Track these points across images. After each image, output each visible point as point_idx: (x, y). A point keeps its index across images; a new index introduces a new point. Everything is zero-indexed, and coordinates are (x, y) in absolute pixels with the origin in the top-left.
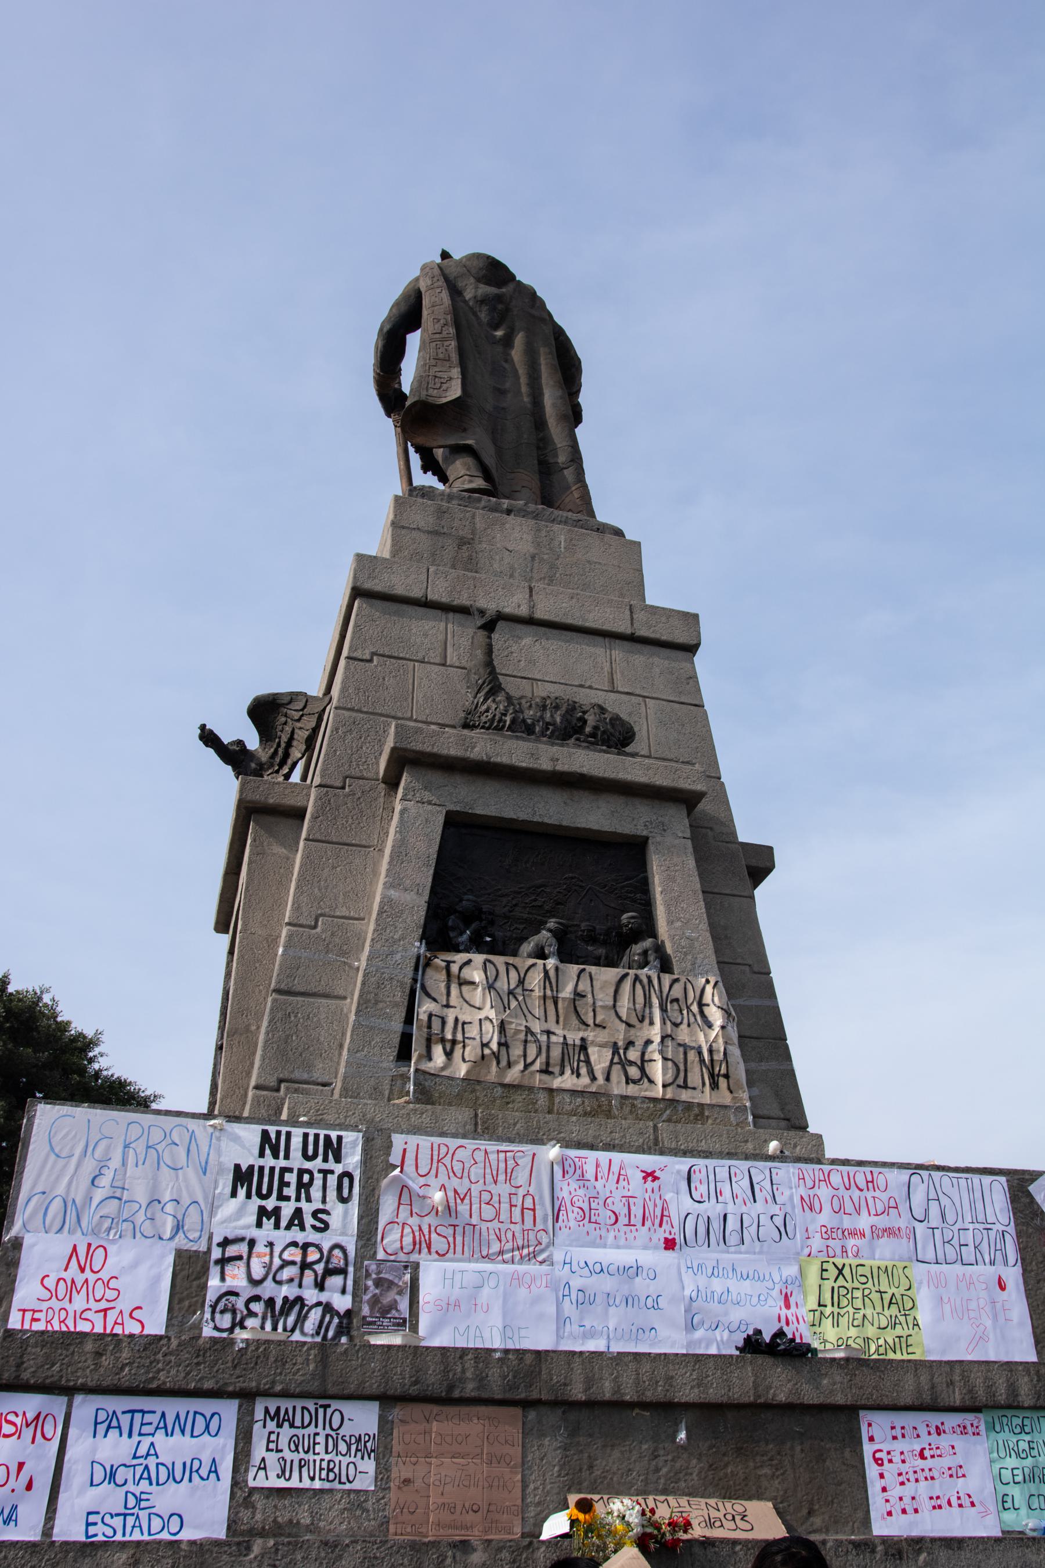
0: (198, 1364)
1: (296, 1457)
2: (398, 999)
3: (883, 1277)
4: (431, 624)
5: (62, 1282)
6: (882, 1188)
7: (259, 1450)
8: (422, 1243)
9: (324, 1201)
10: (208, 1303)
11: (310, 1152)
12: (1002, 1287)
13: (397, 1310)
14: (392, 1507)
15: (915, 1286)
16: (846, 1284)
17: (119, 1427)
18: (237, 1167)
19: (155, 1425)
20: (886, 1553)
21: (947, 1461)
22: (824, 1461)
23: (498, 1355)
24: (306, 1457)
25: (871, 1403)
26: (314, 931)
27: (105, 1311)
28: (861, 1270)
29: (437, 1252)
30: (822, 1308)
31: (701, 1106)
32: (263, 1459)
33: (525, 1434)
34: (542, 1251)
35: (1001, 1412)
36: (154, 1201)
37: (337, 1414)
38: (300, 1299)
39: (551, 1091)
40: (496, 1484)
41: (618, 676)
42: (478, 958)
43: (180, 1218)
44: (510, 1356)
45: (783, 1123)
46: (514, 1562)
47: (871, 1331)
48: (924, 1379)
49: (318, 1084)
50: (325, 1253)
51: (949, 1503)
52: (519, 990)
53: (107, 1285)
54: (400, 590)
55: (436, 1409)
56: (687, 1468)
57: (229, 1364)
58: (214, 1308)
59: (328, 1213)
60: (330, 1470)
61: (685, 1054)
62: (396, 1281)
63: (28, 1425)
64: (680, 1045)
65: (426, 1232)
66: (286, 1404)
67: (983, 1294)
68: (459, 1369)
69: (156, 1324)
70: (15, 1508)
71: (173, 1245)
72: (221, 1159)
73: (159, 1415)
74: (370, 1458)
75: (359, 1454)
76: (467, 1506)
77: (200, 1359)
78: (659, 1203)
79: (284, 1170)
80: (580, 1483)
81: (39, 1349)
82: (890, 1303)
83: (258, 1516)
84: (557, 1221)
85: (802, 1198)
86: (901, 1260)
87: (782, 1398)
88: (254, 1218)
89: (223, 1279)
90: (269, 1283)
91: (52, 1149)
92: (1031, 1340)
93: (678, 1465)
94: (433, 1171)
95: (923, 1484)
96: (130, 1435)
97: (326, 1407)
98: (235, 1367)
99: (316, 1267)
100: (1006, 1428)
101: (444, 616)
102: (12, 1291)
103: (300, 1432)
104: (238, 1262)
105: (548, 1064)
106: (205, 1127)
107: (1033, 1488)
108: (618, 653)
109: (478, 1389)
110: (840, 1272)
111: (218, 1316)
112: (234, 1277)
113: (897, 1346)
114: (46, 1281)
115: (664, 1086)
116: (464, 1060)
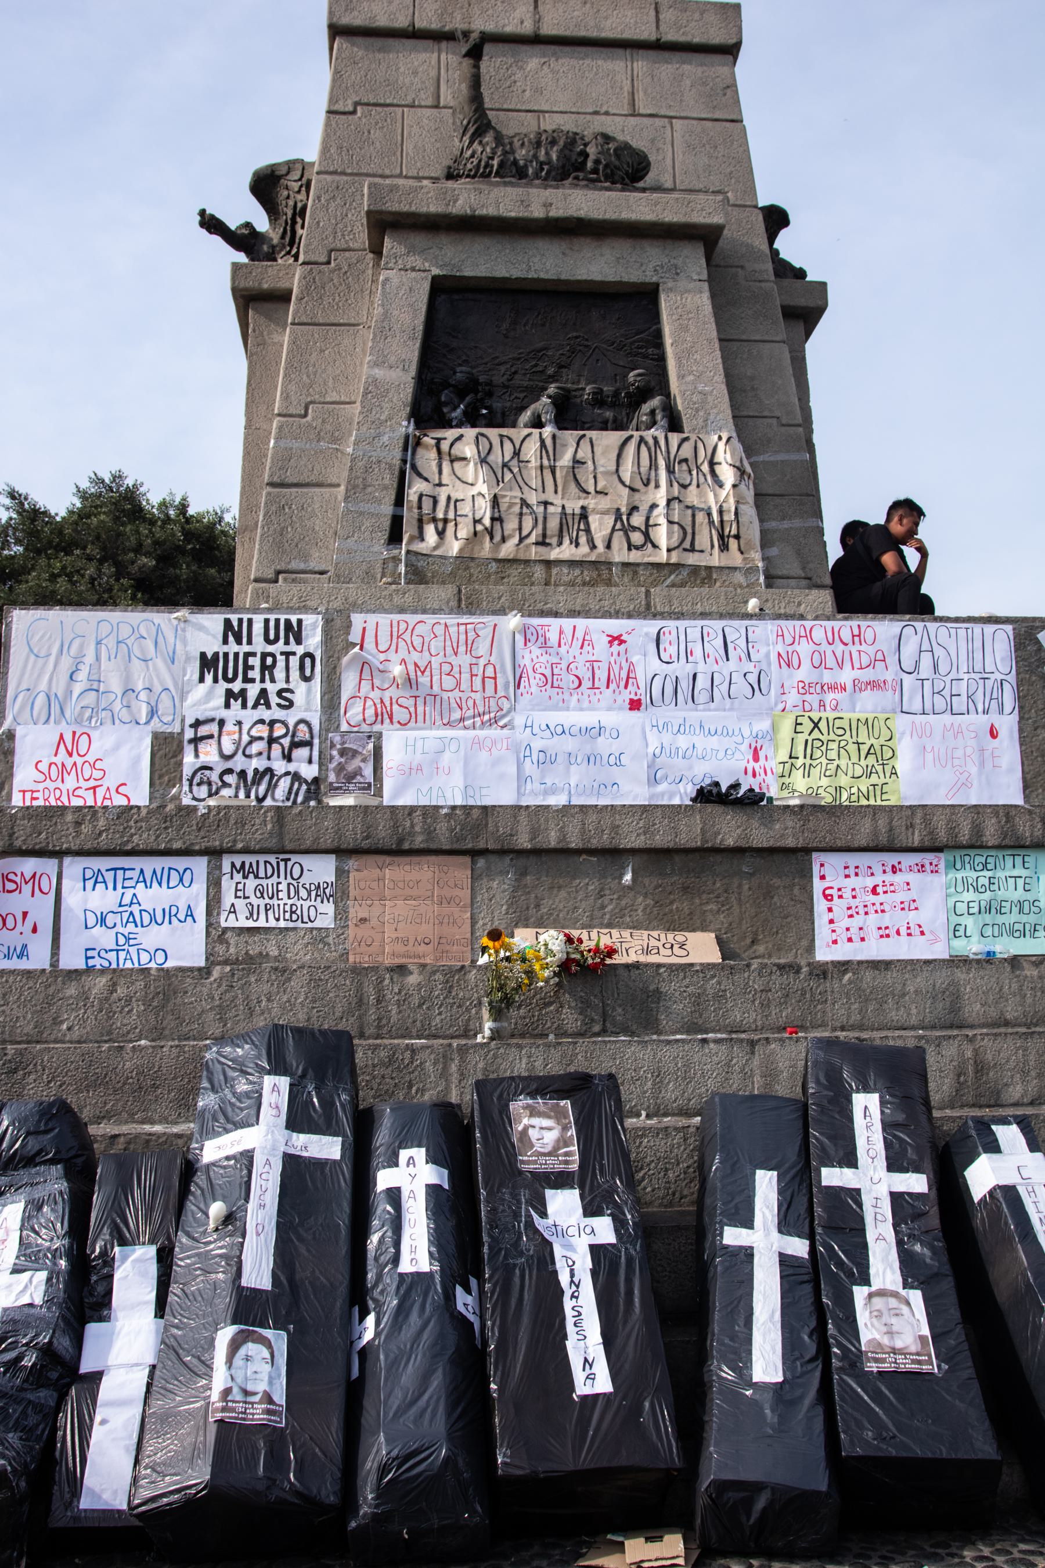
0: (166, 828)
1: (262, 902)
2: (387, 482)
3: (863, 729)
4: (424, 56)
5: (53, 766)
6: (870, 641)
7: (228, 898)
8: (384, 714)
9: (287, 681)
10: (185, 777)
11: (272, 636)
12: (993, 734)
13: (362, 776)
14: (351, 941)
15: (896, 736)
16: (821, 737)
17: (105, 882)
18: (203, 655)
19: (135, 879)
20: (811, 974)
21: (901, 896)
22: (772, 897)
23: (445, 811)
24: (271, 902)
25: (823, 845)
26: (304, 420)
27: (94, 788)
28: (838, 723)
29: (399, 722)
30: (793, 760)
31: (709, 568)
32: (233, 905)
33: (474, 878)
34: (503, 717)
35: (963, 852)
36: (128, 690)
37: (297, 866)
38: (269, 770)
39: (548, 564)
40: (446, 920)
41: (640, 96)
42: (470, 433)
43: (153, 704)
44: (458, 812)
45: (804, 582)
46: (447, 982)
47: (844, 780)
48: (882, 823)
49: (316, 573)
50: (291, 728)
51: (898, 933)
52: (515, 462)
53: (93, 766)
54: (382, 21)
55: (388, 859)
56: (633, 905)
57: (195, 827)
58: (191, 781)
59: (292, 691)
60: (292, 912)
61: (694, 516)
62: (360, 750)
63: (26, 883)
64: (688, 507)
65: (388, 704)
66: (249, 859)
67: (973, 743)
68: (408, 824)
69: (140, 796)
70: (25, 947)
71: (150, 728)
72: (188, 648)
73: (138, 871)
74: (329, 901)
75: (319, 899)
76: (419, 939)
77: (168, 824)
78: (625, 666)
79: (248, 655)
80: (527, 919)
81: (26, 822)
82: (868, 753)
83: (232, 950)
84: (519, 687)
85: (779, 654)
86: (883, 712)
87: (730, 842)
88: (222, 701)
89: (197, 756)
90: (239, 756)
91: (31, 650)
92: (1020, 785)
93: (623, 903)
94: (393, 647)
95: (872, 916)
96: (115, 889)
97: (286, 860)
98: (199, 830)
99: (282, 741)
100: (968, 866)
101: (436, 47)
102: (12, 775)
103: (264, 882)
104: (210, 741)
105: (544, 535)
106: (170, 620)
107: (988, 918)
108: (642, 65)
109: (427, 841)
110: (816, 725)
111: (195, 788)
112: (207, 754)
113: (872, 794)
114: (40, 766)
115: (669, 550)
116: (456, 538)
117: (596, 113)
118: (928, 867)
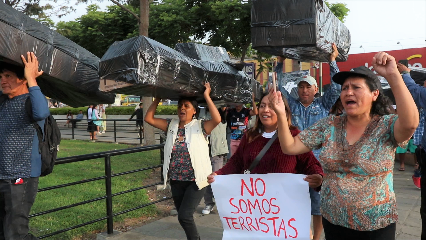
5: (242, 201)
27: (273, 219)
114: (232, 200)
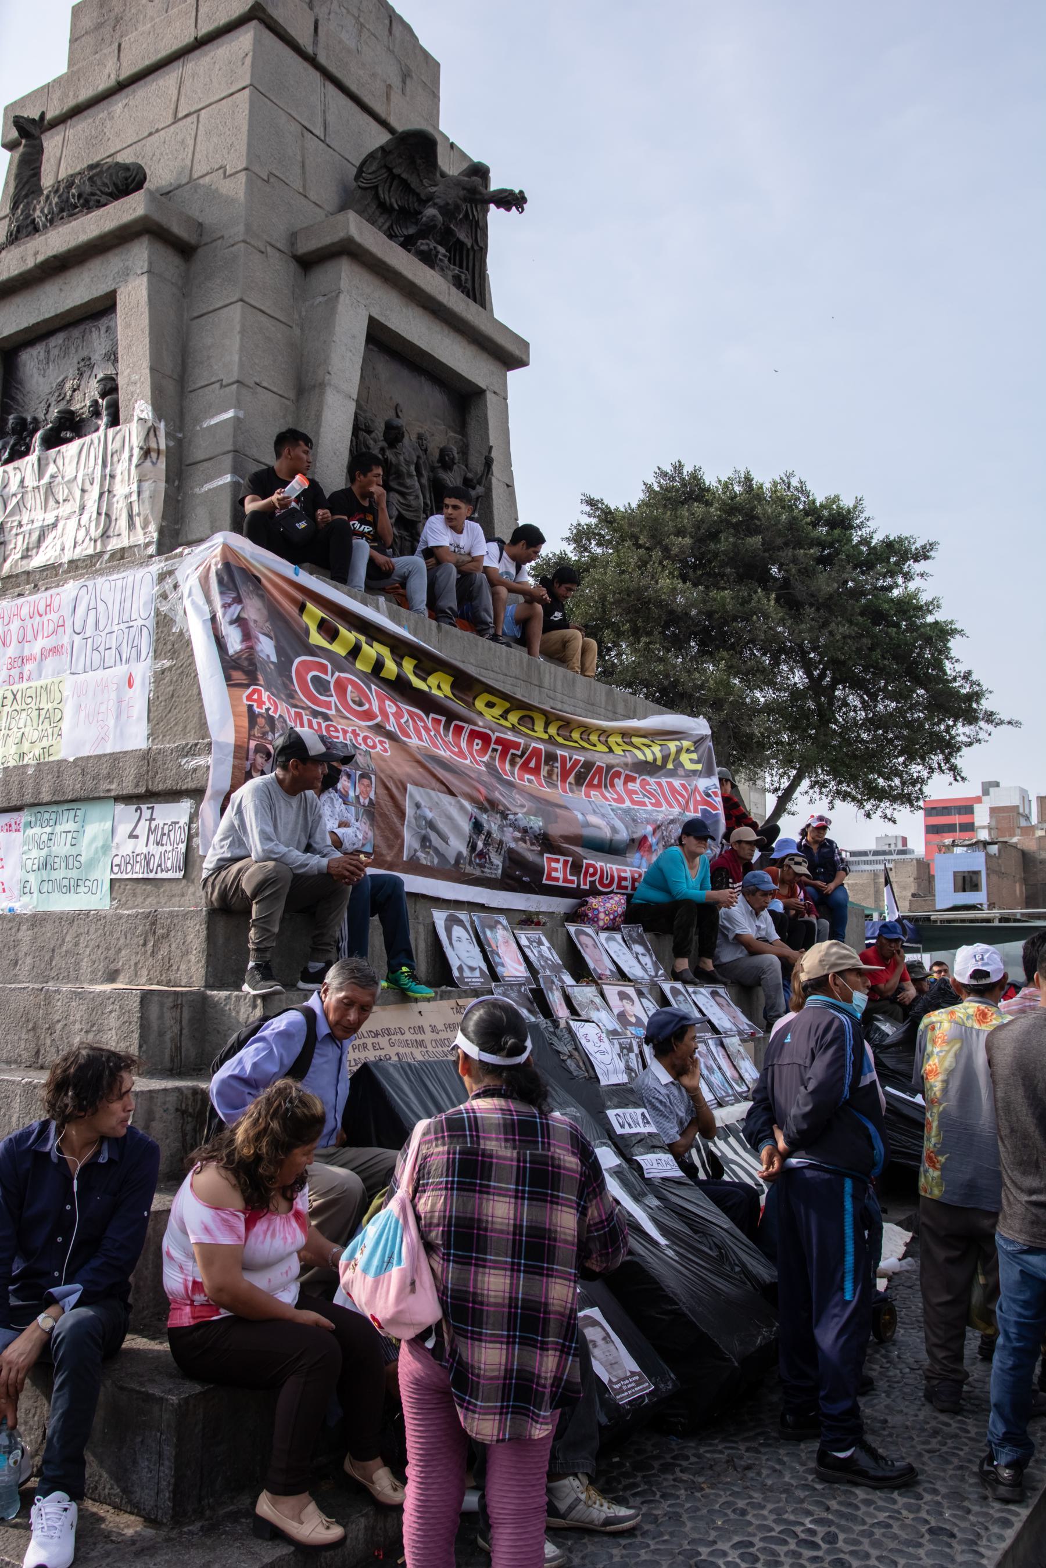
3: (44, 694)
117: (150, 134)
118: (14, 827)
